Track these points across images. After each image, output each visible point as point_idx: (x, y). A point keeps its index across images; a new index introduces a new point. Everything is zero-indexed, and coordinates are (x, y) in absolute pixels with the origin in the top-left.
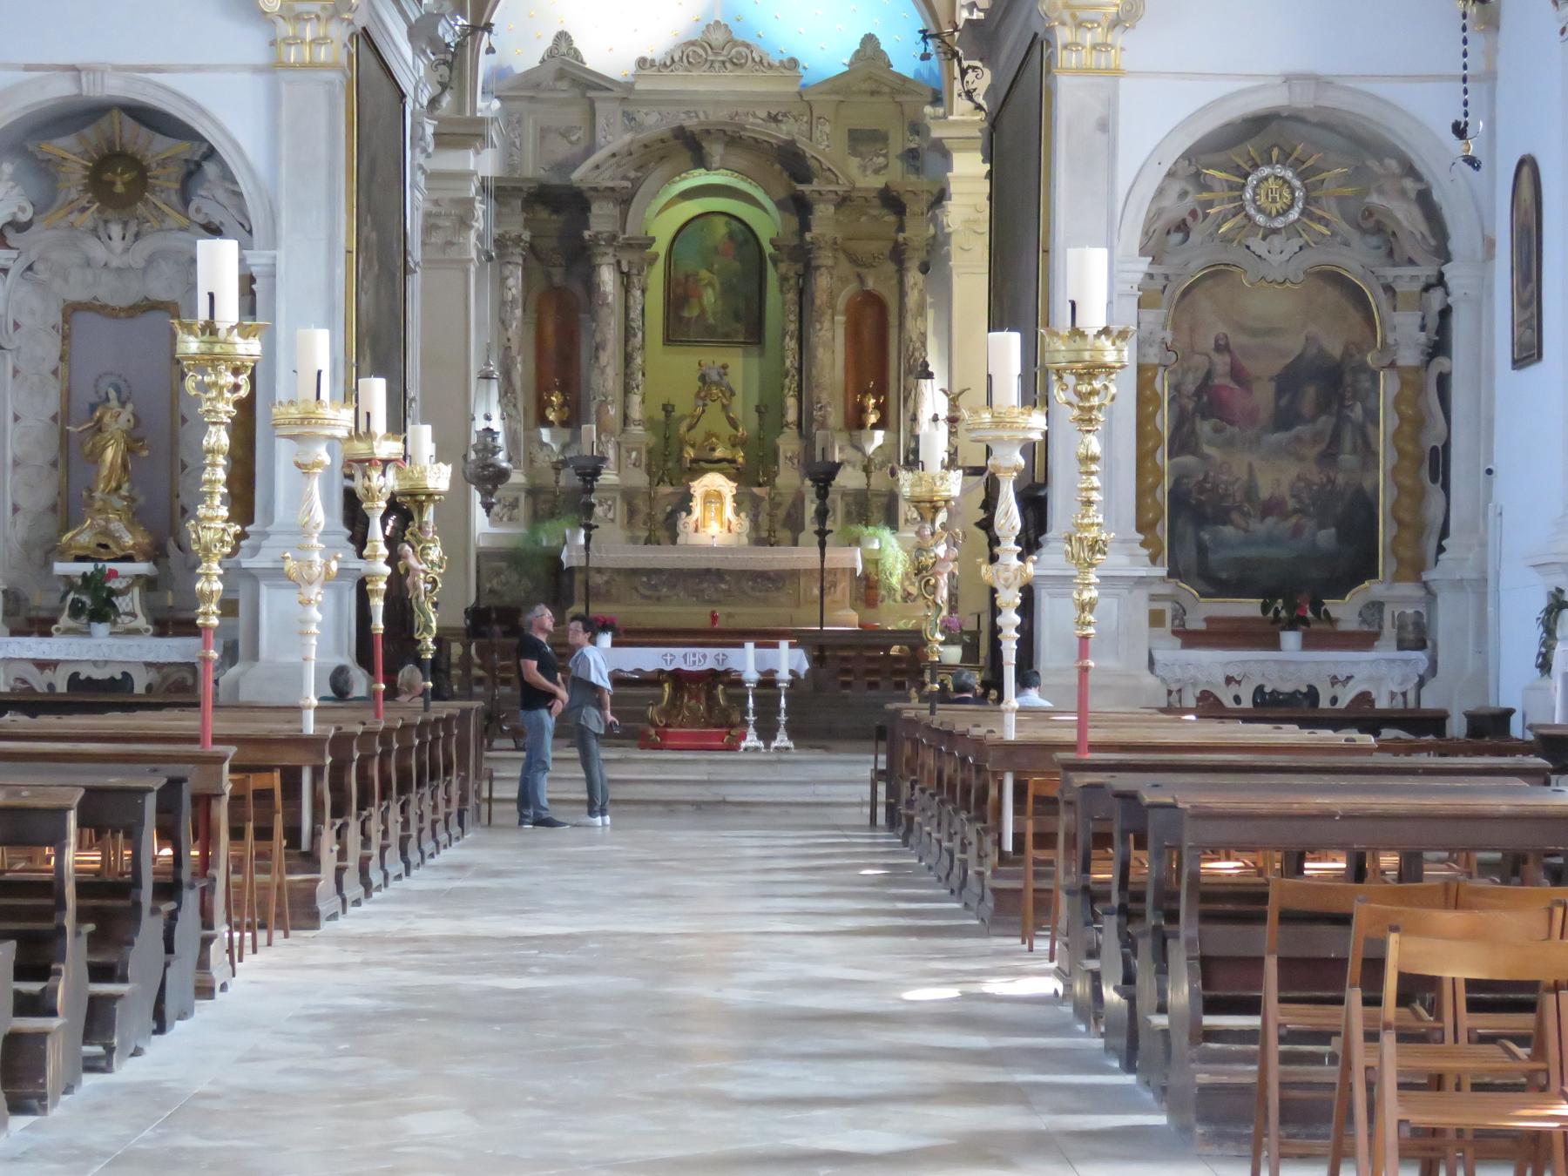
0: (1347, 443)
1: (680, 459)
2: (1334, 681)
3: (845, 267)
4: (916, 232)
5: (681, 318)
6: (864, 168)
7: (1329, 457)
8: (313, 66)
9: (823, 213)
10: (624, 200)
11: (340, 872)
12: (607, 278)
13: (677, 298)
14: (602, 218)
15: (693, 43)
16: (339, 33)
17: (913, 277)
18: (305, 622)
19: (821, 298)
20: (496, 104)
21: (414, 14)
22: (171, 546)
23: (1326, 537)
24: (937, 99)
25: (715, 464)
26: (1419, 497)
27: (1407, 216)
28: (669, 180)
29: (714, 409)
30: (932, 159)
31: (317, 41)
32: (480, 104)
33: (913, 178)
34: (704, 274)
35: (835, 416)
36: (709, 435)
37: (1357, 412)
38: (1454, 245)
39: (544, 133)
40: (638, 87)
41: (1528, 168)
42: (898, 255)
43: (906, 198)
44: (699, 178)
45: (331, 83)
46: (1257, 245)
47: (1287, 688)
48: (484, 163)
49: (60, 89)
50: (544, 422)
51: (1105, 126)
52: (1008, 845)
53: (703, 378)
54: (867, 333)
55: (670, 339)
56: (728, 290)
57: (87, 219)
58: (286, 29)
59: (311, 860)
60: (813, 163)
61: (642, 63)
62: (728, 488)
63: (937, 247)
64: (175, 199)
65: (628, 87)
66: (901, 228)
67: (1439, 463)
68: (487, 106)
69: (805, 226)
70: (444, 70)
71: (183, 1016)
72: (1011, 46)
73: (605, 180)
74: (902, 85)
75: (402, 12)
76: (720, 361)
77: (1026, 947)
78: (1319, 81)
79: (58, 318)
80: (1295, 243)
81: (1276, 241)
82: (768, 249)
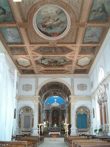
12: (50, 114)
16: (38, 103)
26: (89, 124)
27: (88, 111)
41: (93, 109)
48: (44, 109)
49: (25, 106)
67: (90, 123)
72: (69, 103)
78: (84, 105)
79: (24, 116)
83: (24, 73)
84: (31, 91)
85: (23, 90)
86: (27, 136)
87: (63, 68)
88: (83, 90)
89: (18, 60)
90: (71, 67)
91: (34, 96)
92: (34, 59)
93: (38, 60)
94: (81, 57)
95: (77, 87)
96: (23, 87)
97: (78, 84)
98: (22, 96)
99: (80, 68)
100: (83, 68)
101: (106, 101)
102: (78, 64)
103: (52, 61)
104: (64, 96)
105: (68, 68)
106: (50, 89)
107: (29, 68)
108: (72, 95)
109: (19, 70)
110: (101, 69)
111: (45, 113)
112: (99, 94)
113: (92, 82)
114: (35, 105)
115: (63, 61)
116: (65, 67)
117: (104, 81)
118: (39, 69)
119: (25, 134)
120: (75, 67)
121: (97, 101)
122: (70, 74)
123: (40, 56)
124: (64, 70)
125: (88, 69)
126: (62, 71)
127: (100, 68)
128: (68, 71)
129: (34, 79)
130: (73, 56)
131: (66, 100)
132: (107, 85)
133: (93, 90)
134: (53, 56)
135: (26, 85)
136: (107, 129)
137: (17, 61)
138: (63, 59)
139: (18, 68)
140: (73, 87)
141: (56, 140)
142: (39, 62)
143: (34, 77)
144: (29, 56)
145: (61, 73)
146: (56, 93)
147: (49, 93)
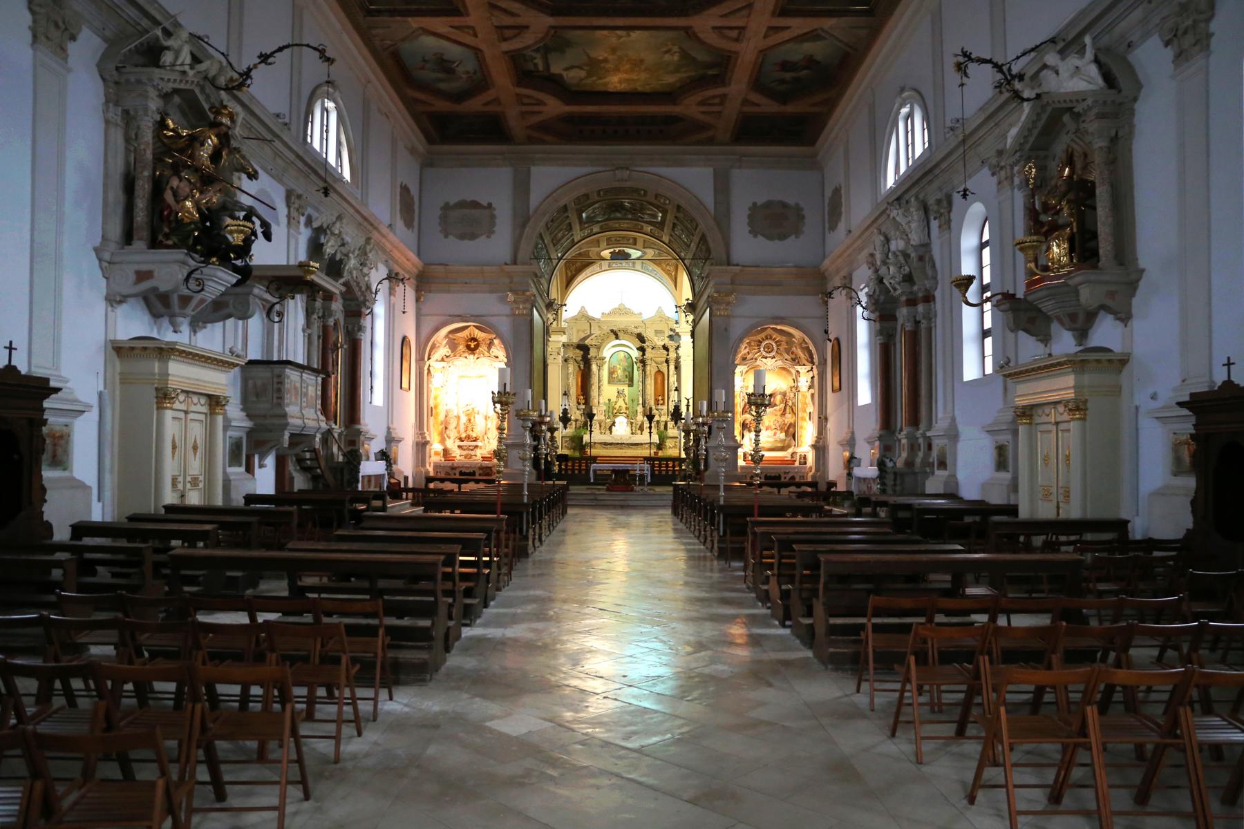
0: (788, 410)
2: (785, 473)
3: (654, 364)
4: (672, 355)
7: (783, 414)
8: (523, 315)
9: (648, 351)
10: (598, 348)
11: (534, 540)
12: (594, 368)
13: (611, 373)
14: (593, 352)
18: (524, 471)
19: (648, 373)
21: (547, 301)
22: (486, 438)
23: (783, 435)
24: (677, 322)
29: (621, 400)
30: (676, 337)
31: (524, 308)
32: (563, 323)
35: (652, 403)
37: (790, 404)
38: (816, 360)
39: (578, 331)
42: (667, 361)
43: (669, 347)
44: (617, 342)
46: (764, 360)
47: (773, 475)
51: (726, 330)
52: (721, 534)
54: (659, 381)
55: (609, 383)
56: (625, 370)
57: (466, 355)
58: (515, 306)
59: (526, 538)
61: (603, 314)
62: (625, 420)
64: (487, 349)
65: (599, 320)
66: (668, 355)
68: (564, 325)
69: (644, 354)
71: (493, 599)
74: (668, 319)
77: (728, 565)
80: (774, 360)
81: (769, 359)
82: (634, 360)
83: (446, 138)
84: (488, 237)
85: (446, 237)
86: (477, 481)
87: (675, 104)
88: (783, 237)
90: (723, 97)
92: (506, 46)
93: (529, 53)
94: (786, 35)
95: (750, 216)
96: (444, 219)
97: (755, 204)
98: (441, 268)
101: (929, 298)
103: (611, 57)
104: (669, 274)
105: (702, 103)
106: (596, 229)
107: (475, 105)
108: (721, 265)
109: (416, 117)
110: (905, 110)
112: (878, 257)
113: (837, 191)
114: (514, 315)
115: (676, 58)
117: (925, 181)
118: (536, 108)
119: (464, 470)
120: (746, 102)
121: (869, 296)
122: (711, 141)
123: (540, 23)
127: (900, 109)
128: (699, 127)
130: (740, 24)
132: (945, 203)
133: (838, 239)
134: (620, 21)
135: (462, 205)
136: (921, 454)
137: (396, 56)
138: (676, 49)
139: (409, 104)
140: (722, 219)
141: (631, 503)
142: (531, 67)
144: (469, 21)
146: (626, 257)
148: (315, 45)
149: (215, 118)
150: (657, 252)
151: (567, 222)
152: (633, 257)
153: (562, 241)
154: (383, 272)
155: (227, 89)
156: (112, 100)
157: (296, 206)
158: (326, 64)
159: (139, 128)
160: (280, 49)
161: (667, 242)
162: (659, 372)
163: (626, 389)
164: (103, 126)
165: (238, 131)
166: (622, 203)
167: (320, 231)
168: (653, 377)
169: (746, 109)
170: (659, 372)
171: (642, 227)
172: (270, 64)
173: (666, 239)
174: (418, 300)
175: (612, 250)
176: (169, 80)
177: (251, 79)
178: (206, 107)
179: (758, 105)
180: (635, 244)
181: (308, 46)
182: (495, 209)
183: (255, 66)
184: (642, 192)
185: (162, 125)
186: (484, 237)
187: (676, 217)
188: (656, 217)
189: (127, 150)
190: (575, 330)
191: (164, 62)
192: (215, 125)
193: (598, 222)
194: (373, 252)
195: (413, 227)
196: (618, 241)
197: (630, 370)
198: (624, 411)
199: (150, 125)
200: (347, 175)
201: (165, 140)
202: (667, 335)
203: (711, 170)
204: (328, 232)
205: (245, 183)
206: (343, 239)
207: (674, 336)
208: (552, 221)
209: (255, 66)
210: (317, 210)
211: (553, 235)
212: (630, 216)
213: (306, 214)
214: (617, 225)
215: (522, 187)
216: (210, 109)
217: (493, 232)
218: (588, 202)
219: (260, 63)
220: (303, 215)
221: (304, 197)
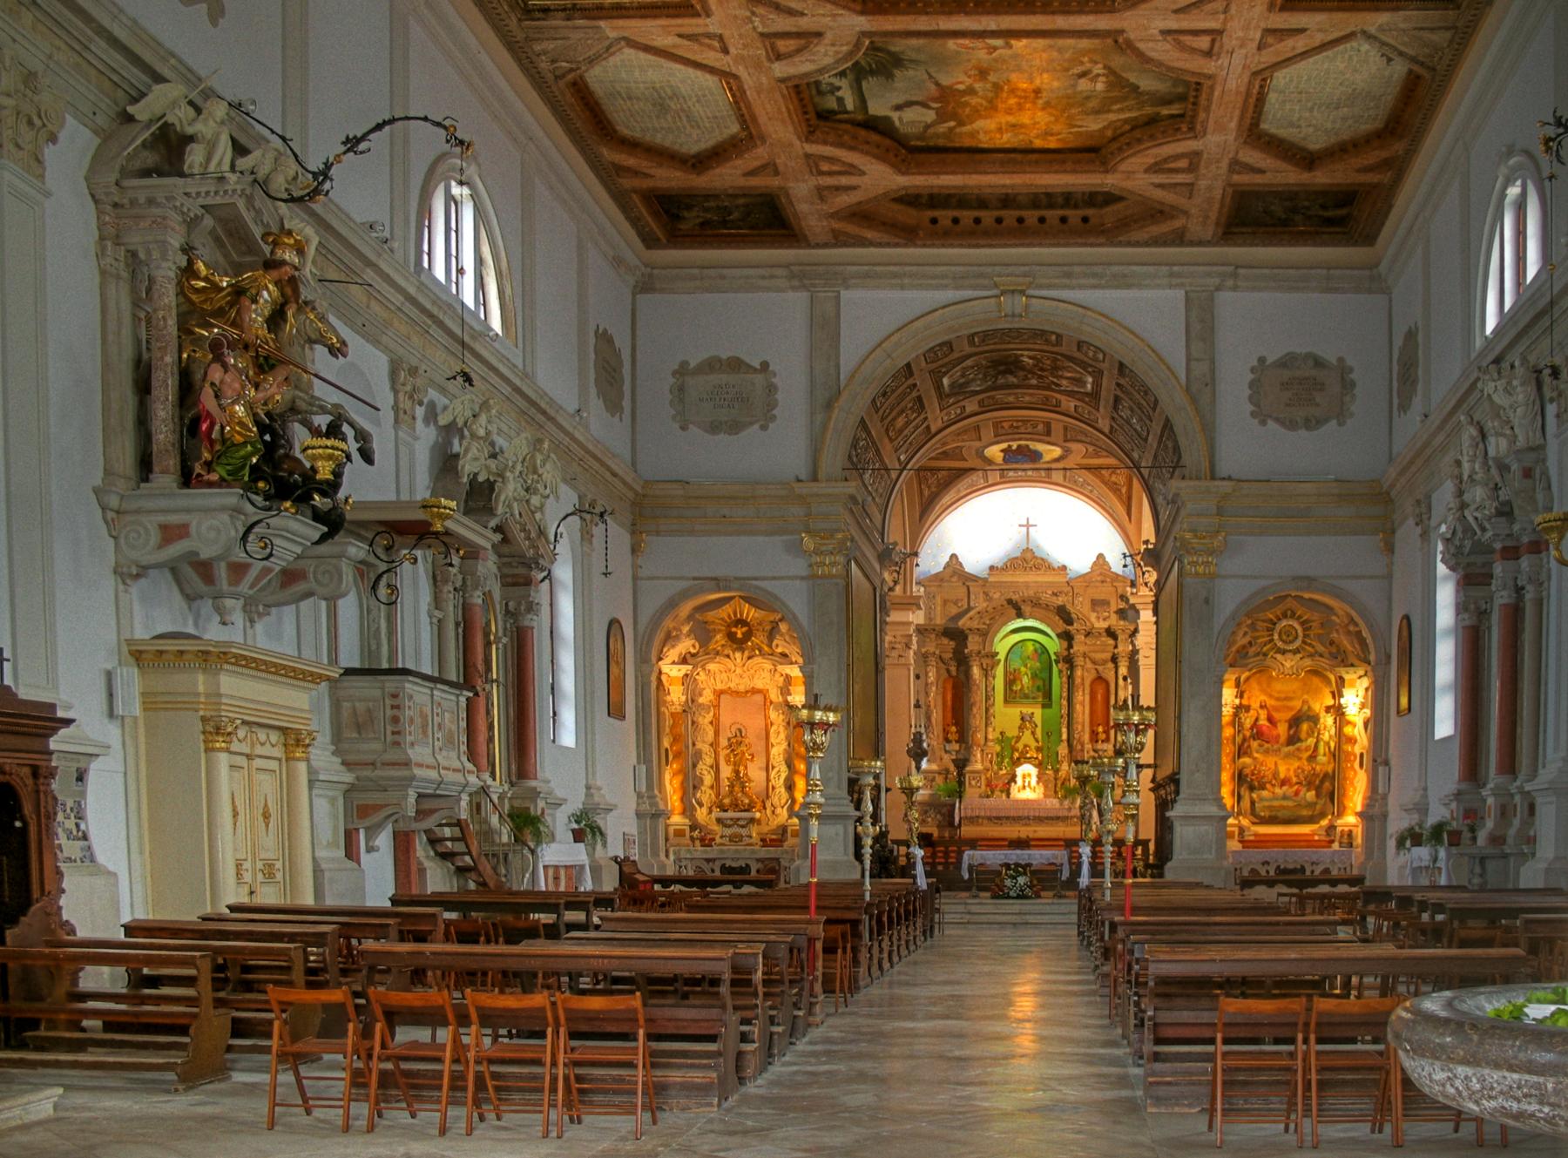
1: (1012, 758)
3: (1089, 665)
4: (1124, 648)
5: (1011, 690)
6: (1098, 618)
9: (1079, 638)
10: (986, 634)
12: (976, 671)
13: (1011, 680)
14: (973, 644)
15: (1016, 558)
17: (1123, 671)
19: (1078, 681)
20: (922, 589)
21: (880, 548)
25: (1029, 760)
28: (1005, 624)
29: (1028, 733)
30: (1131, 613)
33: (1122, 623)
34: (1023, 669)
35: (1086, 737)
36: (1025, 746)
39: (945, 602)
40: (991, 579)
42: (1114, 659)
43: (1118, 632)
45: (837, 584)
48: (917, 617)
50: (947, 741)
53: (1022, 719)
55: (1006, 701)
56: (1034, 676)
60: (1074, 616)
61: (992, 568)
63: (1133, 656)
65: (985, 580)
66: (1116, 647)
68: (919, 591)
69: (1070, 646)
70: (895, 575)
73: (975, 625)
75: (874, 547)
76: (1030, 711)
82: (1053, 657)
84: (764, 428)
87: (1107, 172)
89: (597, 77)
91: (799, 489)
99: (1286, 176)
100: (1321, 178)
102: (1264, 126)
104: (1115, 488)
106: (971, 406)
111: (923, 658)
116: (1123, 167)
122: (1179, 238)
124: (1110, 199)
125: (1375, 186)
126: (1089, 212)
128: (1158, 213)
129: (797, 301)
131: (1131, 528)
143: (792, 276)
145: (1088, 231)
146: (1035, 456)
147: (957, 454)
148: (439, 119)
149: (272, 252)
150: (1091, 449)
151: (914, 394)
152: (1047, 458)
153: (906, 432)
154: (568, 498)
155: (292, 200)
156: (110, 237)
157: (408, 388)
158: (458, 150)
159: (151, 280)
160: (379, 127)
161: (1106, 430)
162: (1100, 679)
163: (1038, 713)
164: (97, 280)
165: (308, 270)
166: (1017, 356)
167: (450, 430)
168: (1087, 691)
169: (1236, 178)
170: (1100, 679)
171: (1058, 404)
172: (361, 153)
173: (1104, 424)
174: (635, 550)
175: (1004, 446)
176: (198, 194)
177: (332, 180)
178: (257, 232)
179: (1261, 171)
180: (1048, 433)
181: (425, 119)
182: (775, 375)
183: (338, 158)
184: (1054, 337)
185: (189, 271)
186: (756, 426)
187: (1118, 385)
188: (1085, 383)
189: (134, 315)
190: (939, 600)
191: (190, 167)
192: (271, 264)
193: (977, 393)
194: (548, 466)
195: (622, 413)
196: (1014, 431)
197: (1045, 675)
198: (1032, 753)
199: (172, 275)
200: (496, 323)
201: (194, 297)
202: (1114, 607)
203: (1180, 294)
204: (466, 433)
205: (319, 357)
206: (492, 444)
207: (1128, 612)
208: (884, 394)
209: (338, 158)
210: (443, 391)
211: (886, 422)
212: (1034, 382)
213: (425, 401)
214: (1011, 399)
215: (825, 330)
216: (265, 236)
217: (774, 418)
218: (956, 355)
219: (345, 153)
220: (421, 403)
221: (421, 371)
